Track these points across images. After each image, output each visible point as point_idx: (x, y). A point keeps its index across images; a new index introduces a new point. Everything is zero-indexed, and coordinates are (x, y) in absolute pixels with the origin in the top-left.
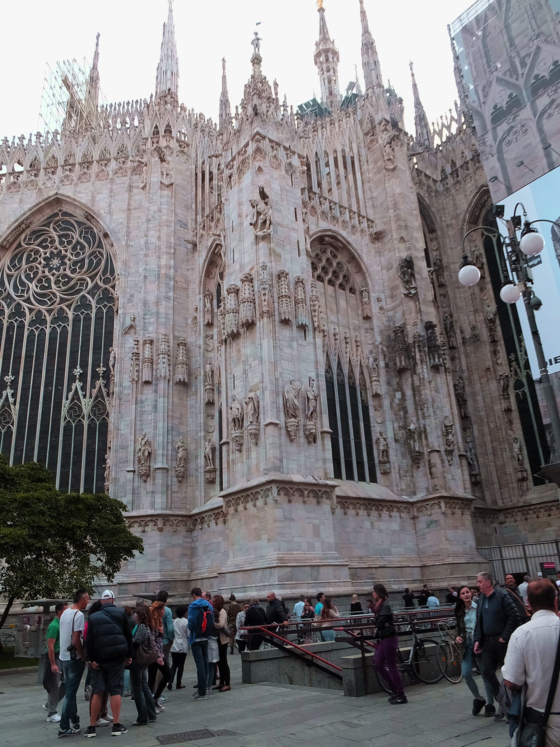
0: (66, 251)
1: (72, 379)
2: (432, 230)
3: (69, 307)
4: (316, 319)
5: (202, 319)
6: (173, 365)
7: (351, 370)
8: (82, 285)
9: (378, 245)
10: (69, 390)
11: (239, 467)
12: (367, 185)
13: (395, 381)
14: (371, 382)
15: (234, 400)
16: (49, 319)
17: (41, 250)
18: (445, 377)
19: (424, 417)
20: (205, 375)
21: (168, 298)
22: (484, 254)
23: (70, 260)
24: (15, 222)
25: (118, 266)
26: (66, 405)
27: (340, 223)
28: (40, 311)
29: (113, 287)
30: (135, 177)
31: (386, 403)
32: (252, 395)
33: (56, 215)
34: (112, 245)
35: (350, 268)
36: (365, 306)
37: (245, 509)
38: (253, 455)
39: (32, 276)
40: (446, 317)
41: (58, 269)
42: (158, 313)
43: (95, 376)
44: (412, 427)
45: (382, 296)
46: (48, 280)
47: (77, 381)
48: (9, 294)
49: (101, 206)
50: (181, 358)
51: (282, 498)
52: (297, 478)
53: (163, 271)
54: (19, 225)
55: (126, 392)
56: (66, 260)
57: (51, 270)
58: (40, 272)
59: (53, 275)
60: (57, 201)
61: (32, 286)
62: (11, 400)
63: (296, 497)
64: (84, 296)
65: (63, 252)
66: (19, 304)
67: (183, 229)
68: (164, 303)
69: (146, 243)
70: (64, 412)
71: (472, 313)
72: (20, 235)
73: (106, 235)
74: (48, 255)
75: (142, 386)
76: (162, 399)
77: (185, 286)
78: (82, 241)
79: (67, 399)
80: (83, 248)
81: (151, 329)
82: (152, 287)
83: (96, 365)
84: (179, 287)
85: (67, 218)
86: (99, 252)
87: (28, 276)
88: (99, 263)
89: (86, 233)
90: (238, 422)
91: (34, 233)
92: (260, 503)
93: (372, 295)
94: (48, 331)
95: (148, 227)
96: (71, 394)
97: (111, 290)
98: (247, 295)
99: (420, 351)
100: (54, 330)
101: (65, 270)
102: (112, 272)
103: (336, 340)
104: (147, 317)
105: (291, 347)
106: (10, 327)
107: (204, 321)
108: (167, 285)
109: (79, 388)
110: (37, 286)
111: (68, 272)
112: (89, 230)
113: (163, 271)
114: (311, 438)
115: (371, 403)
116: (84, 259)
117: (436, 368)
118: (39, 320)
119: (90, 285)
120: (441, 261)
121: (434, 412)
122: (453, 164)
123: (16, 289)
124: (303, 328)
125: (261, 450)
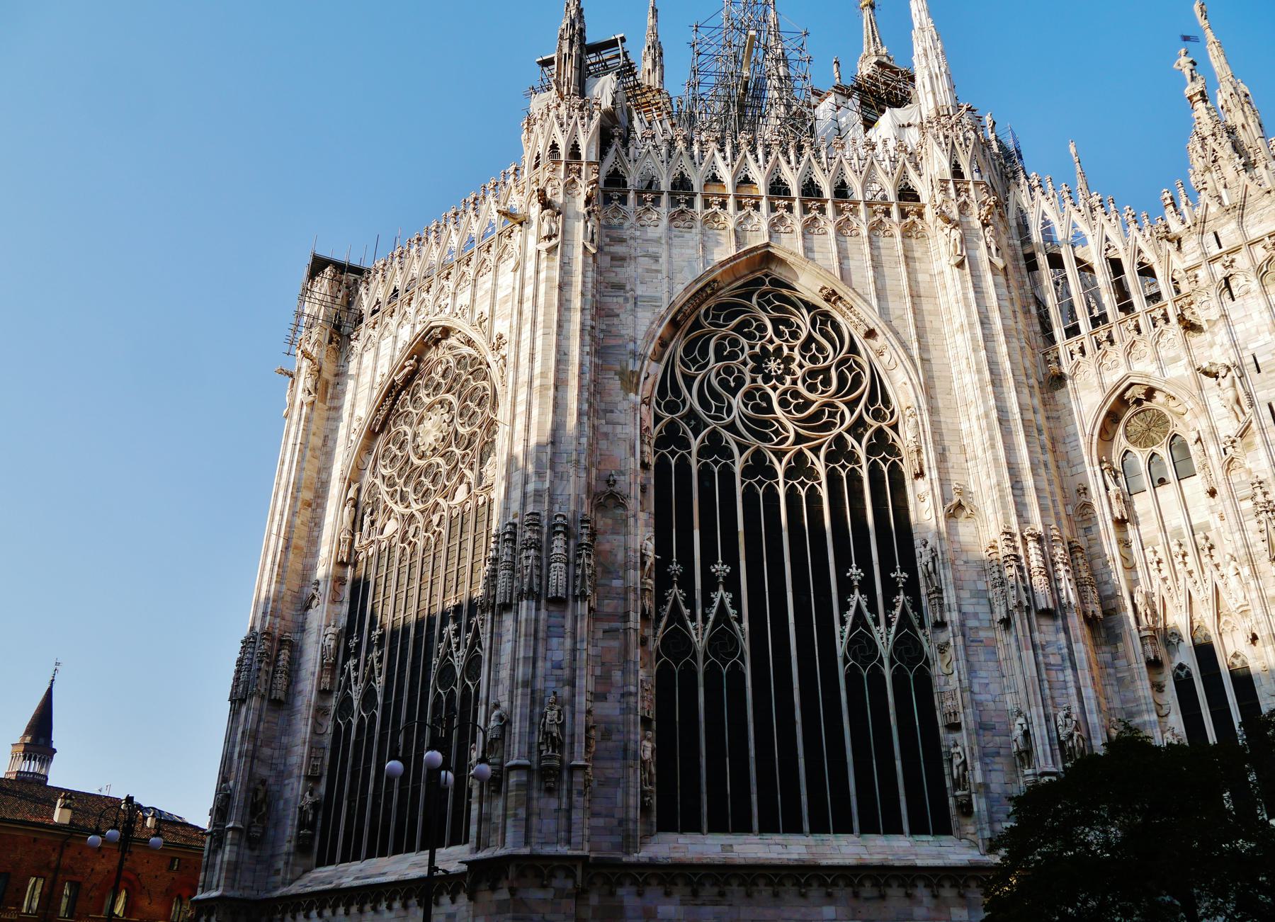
0: (791, 349)
1: (846, 587)
3: (816, 450)
8: (832, 415)
10: (844, 607)
16: (780, 470)
17: (744, 341)
24: (697, 281)
26: (846, 634)
29: (895, 427)
33: (758, 282)
41: (781, 379)
43: (890, 588)
47: (857, 591)
48: (692, 409)
54: (702, 289)
55: (971, 623)
56: (794, 366)
57: (767, 379)
58: (748, 380)
59: (775, 388)
60: (766, 257)
61: (737, 402)
62: (732, 612)
64: (840, 436)
65: (786, 351)
70: (841, 649)
72: (699, 305)
74: (757, 349)
78: (818, 336)
79: (843, 622)
83: (887, 566)
85: (785, 292)
86: (855, 362)
87: (724, 383)
88: (857, 381)
89: (823, 323)
91: (720, 307)
94: (781, 491)
96: (850, 614)
101: (794, 382)
102: (886, 401)
106: (705, 472)
109: (863, 604)
110: (746, 405)
111: (801, 387)
116: (829, 368)
118: (758, 466)
119: (849, 420)
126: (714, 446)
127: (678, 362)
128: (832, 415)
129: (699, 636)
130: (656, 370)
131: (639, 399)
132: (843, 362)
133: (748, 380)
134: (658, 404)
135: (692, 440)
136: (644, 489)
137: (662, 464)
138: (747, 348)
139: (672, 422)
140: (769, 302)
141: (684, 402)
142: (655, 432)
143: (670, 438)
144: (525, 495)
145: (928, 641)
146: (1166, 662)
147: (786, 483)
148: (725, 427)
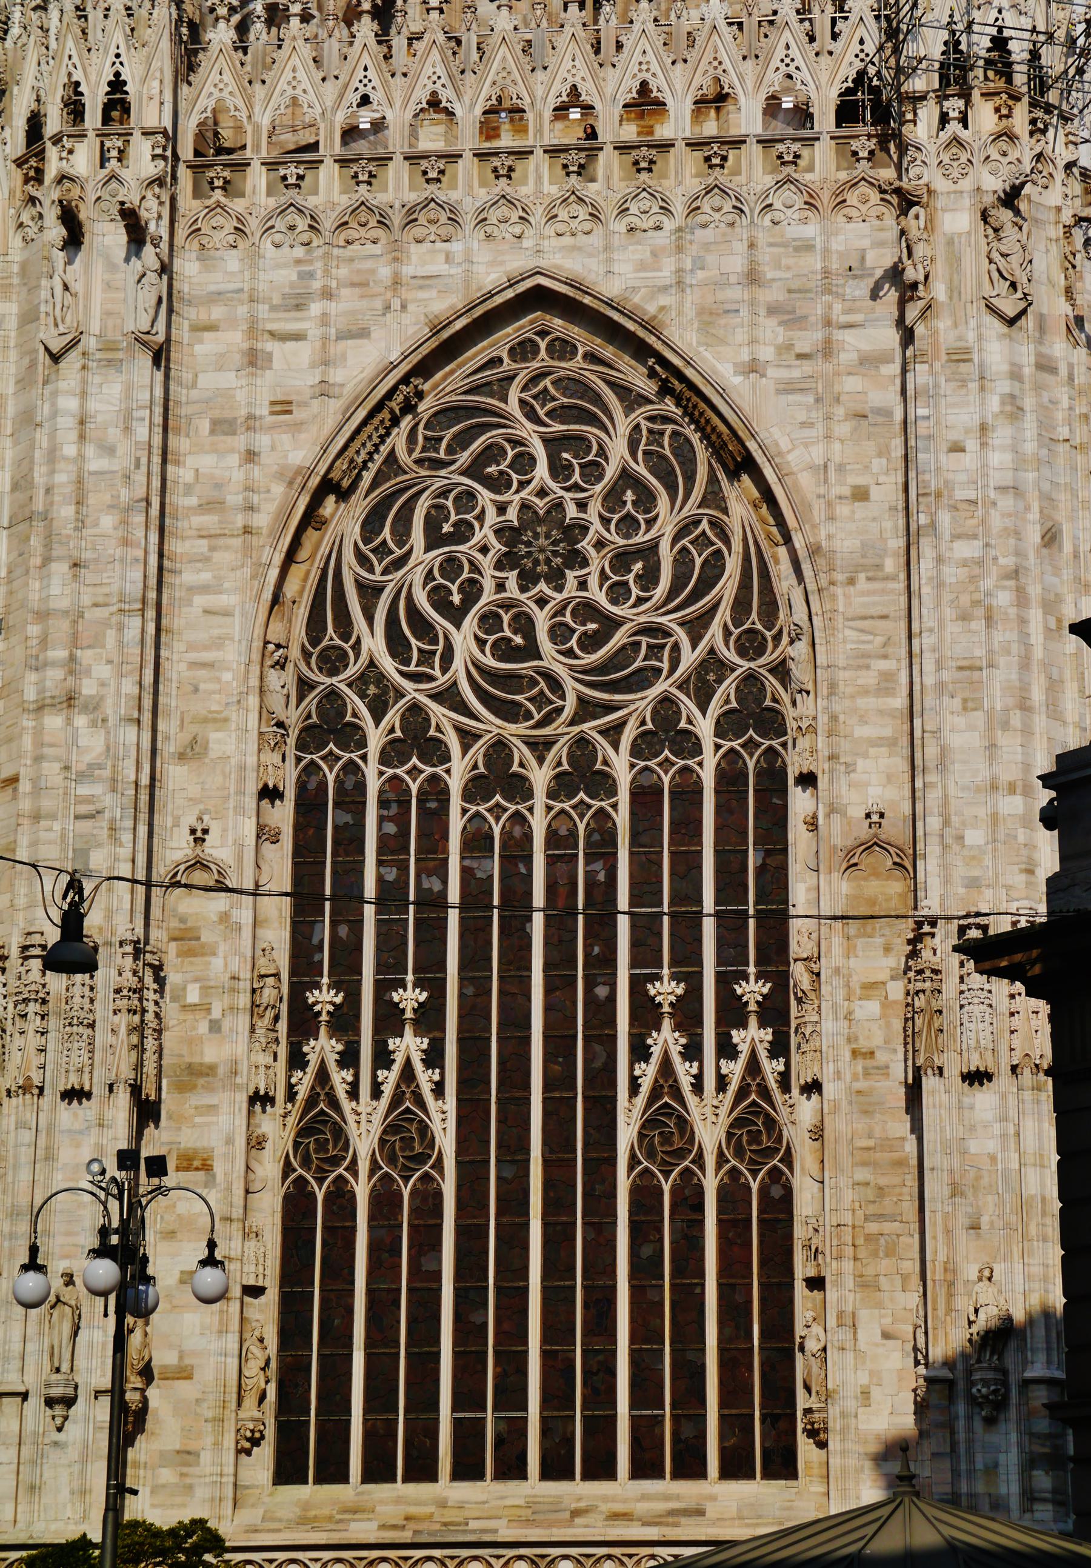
8: (655, 651)
16: (540, 777)
17: (485, 496)
39: (456, 599)
48: (372, 663)
58: (488, 585)
61: (463, 637)
64: (666, 701)
65: (572, 511)
66: (415, 708)
80: (646, 500)
94: (539, 824)
96: (648, 1072)
97: (772, 682)
101: (583, 585)
106: (394, 796)
110: (481, 643)
119: (689, 658)
123: (397, 646)
126: (416, 740)
127: (349, 556)
129: (365, 1128)
140: (544, 396)
145: (799, 1115)
147: (549, 808)
148: (435, 697)
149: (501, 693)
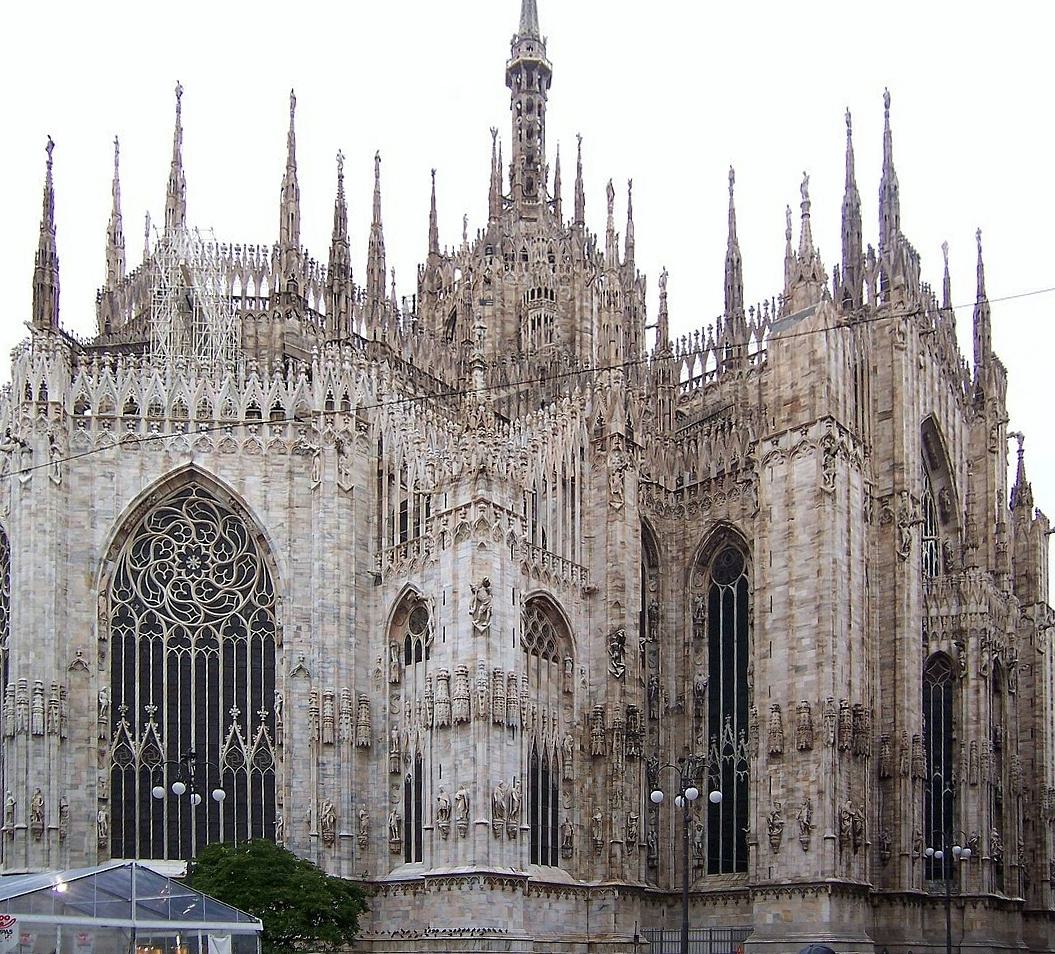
0: (207, 549)
2: (654, 566)
3: (217, 626)
4: (524, 718)
5: (387, 676)
6: (356, 725)
7: (546, 754)
8: (231, 600)
9: (589, 602)
11: (443, 852)
12: (587, 517)
13: (588, 764)
14: (564, 765)
15: (442, 792)
16: (193, 640)
18: (638, 766)
19: (612, 809)
20: (391, 741)
21: (349, 645)
22: (707, 605)
23: (213, 563)
25: (279, 588)
27: (552, 580)
28: (179, 626)
29: (272, 609)
30: (298, 458)
31: (577, 789)
32: (463, 792)
34: (268, 551)
35: (555, 631)
36: (567, 680)
37: (449, 890)
38: (461, 845)
39: (165, 577)
40: (652, 682)
42: (338, 662)
44: (599, 816)
45: (586, 667)
46: (187, 588)
48: (136, 596)
49: (252, 497)
50: (363, 718)
51: (487, 886)
52: (499, 870)
53: (344, 610)
58: (176, 574)
59: (193, 580)
61: (167, 591)
63: (497, 886)
65: (203, 551)
67: (362, 552)
68: (344, 651)
69: (322, 568)
71: (681, 679)
73: (261, 537)
74: (183, 550)
75: (323, 747)
76: (345, 764)
77: (365, 627)
80: (229, 548)
81: (330, 680)
82: (330, 628)
84: (358, 630)
88: (251, 574)
90: (445, 812)
92: (465, 887)
93: (576, 666)
95: (324, 547)
98: (462, 692)
99: (618, 740)
100: (200, 656)
101: (207, 575)
103: (533, 720)
104: (326, 665)
105: (501, 749)
106: (144, 643)
107: (390, 678)
108: (348, 627)
110: (173, 593)
112: (235, 522)
113: (344, 610)
114: (512, 835)
115: (561, 786)
117: (630, 758)
120: (657, 608)
121: (622, 804)
122: (694, 476)
124: (512, 728)
125: (469, 842)
126: (151, 624)
127: (128, 558)
128: (231, 600)
130: (113, 567)
131: (97, 593)
132: (243, 558)
133: (176, 574)
134: (115, 593)
135: (136, 620)
136: (102, 655)
137: (116, 638)
138: (176, 548)
139: (124, 606)
141: (132, 591)
142: (111, 615)
143: (123, 618)
144: (19, 666)
146: (402, 773)
149: (180, 610)
